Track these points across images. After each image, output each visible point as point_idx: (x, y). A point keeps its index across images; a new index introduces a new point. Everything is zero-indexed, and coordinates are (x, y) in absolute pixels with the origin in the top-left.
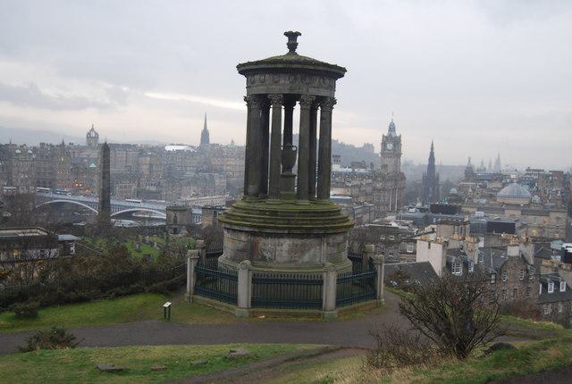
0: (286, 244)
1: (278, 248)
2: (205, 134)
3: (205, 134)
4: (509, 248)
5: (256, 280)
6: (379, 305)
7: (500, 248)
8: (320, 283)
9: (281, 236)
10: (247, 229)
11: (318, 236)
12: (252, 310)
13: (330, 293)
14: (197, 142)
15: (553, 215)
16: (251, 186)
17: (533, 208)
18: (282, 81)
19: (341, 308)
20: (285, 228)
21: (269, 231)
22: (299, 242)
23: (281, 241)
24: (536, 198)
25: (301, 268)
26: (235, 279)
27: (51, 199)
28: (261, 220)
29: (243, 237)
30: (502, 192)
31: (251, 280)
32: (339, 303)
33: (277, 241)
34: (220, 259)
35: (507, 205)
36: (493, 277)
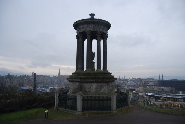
0: (95, 85)
1: (91, 87)
2: (59, 73)
3: (59, 73)
4: (139, 93)
5: (84, 100)
6: (129, 108)
7: (137, 94)
8: (110, 99)
9: (92, 82)
10: (79, 80)
11: (106, 82)
12: (83, 112)
13: (114, 103)
14: (58, 75)
15: (140, 88)
16: (79, 65)
17: (135, 86)
18: (90, 26)
19: (120, 109)
20: (94, 79)
21: (88, 80)
22: (99, 84)
23: (93, 84)
24: (136, 84)
25: (100, 95)
26: (75, 99)
27: (23, 88)
28: (85, 77)
29: (77, 84)
30: (128, 83)
31: (82, 100)
32: (118, 107)
33: (91, 84)
34: (68, 94)
35: (130, 86)
36: (136, 101)
